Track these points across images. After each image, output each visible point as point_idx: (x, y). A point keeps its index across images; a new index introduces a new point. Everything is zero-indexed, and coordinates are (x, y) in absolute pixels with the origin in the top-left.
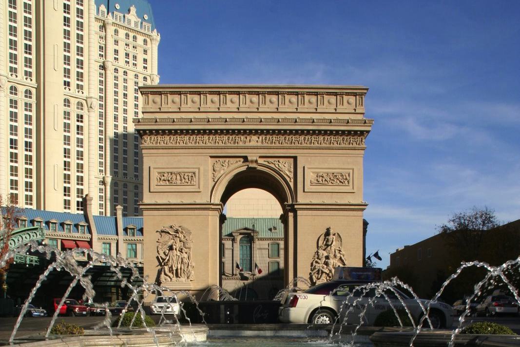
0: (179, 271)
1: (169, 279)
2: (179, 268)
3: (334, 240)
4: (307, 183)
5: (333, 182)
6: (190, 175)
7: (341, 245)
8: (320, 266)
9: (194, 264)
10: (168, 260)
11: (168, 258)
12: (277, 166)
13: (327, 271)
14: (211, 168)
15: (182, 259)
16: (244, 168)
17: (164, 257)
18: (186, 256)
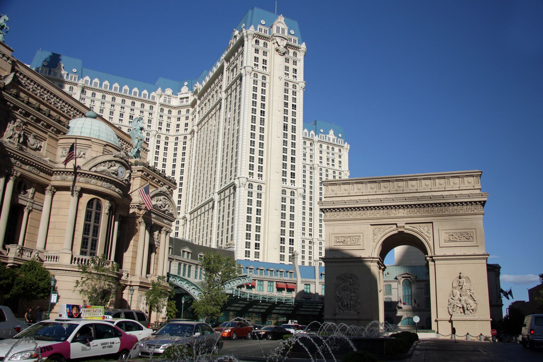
0: (349, 306)
1: (342, 311)
2: (349, 303)
3: (464, 282)
4: (442, 240)
5: (461, 239)
6: (357, 237)
7: (471, 285)
8: (456, 302)
9: (359, 301)
10: (342, 297)
11: (341, 296)
12: (419, 229)
13: (460, 305)
14: (371, 233)
15: (351, 297)
16: (396, 232)
17: (338, 296)
18: (353, 294)
